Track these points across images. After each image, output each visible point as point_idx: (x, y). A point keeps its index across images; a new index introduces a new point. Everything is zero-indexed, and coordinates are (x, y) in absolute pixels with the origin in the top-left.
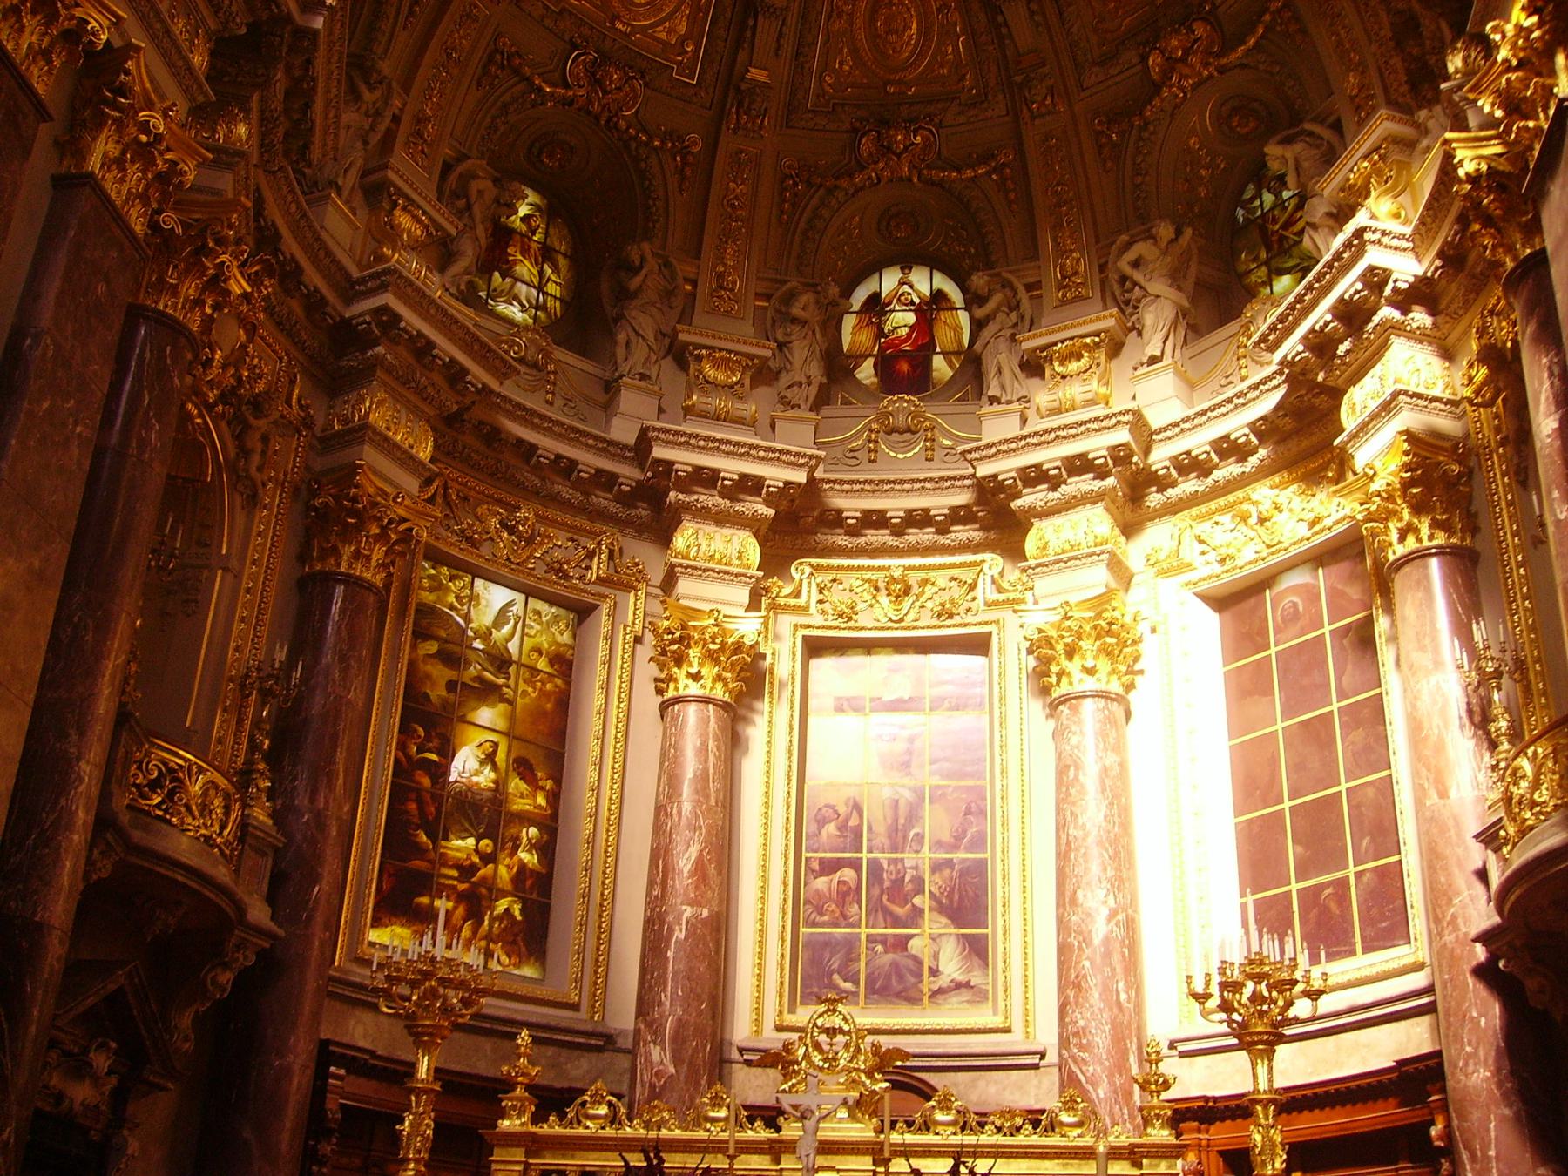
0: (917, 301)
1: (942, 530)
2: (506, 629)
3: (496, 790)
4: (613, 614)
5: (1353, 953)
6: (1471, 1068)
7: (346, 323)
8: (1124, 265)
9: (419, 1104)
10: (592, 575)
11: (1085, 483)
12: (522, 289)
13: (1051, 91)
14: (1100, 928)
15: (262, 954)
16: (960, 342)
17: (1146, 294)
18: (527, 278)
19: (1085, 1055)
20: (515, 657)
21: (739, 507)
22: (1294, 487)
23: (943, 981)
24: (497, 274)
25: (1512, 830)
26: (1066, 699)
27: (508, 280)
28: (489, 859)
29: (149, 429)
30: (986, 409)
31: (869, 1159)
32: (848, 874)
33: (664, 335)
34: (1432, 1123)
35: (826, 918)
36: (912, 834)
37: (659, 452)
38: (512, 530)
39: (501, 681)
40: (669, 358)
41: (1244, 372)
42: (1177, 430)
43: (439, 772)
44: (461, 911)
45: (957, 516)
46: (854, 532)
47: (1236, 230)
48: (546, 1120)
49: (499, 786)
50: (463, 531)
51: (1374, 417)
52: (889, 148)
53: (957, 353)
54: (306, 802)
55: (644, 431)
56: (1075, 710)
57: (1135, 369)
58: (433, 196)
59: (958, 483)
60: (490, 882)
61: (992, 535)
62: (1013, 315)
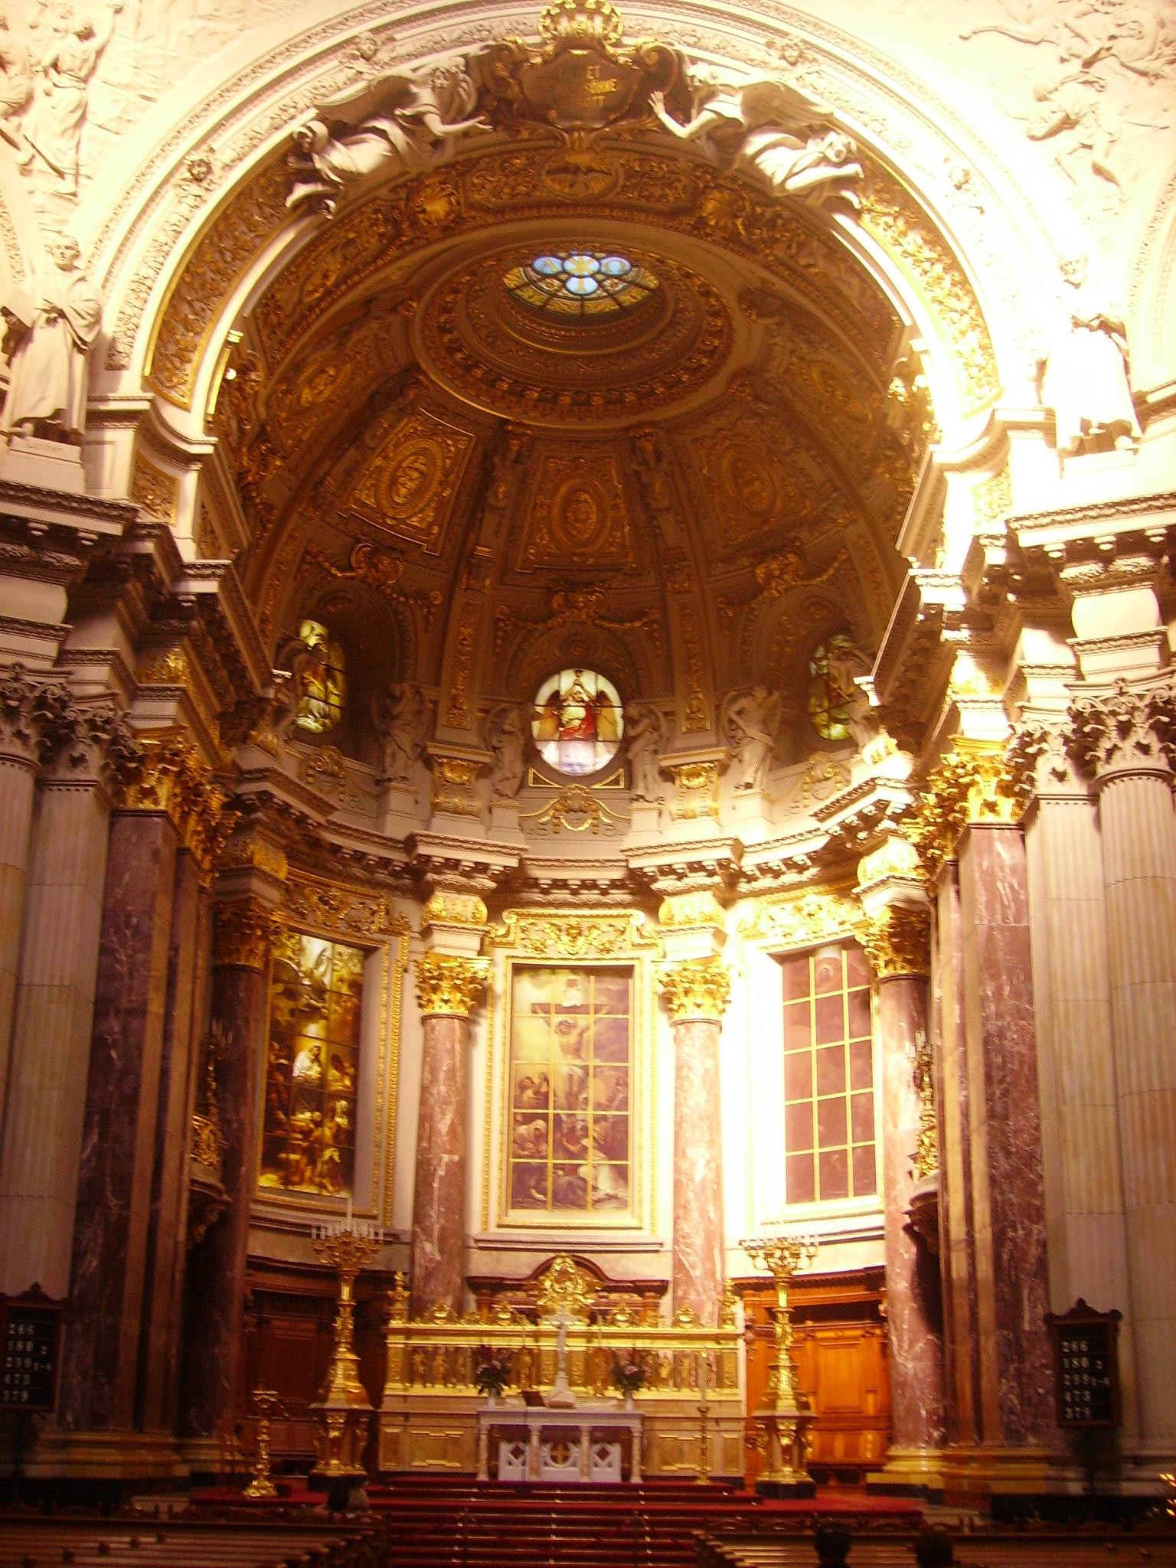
0: (586, 699)
2: (322, 969)
5: (846, 1195)
11: (700, 878)
13: (689, 577)
14: (700, 1173)
15: (222, 1214)
16: (615, 733)
17: (746, 736)
22: (831, 897)
23: (600, 1195)
26: (683, 1023)
28: (319, 1124)
30: (636, 805)
32: (540, 1124)
34: (880, 1302)
37: (423, 850)
38: (326, 903)
39: (320, 1005)
43: (288, 1070)
44: (304, 1160)
45: (614, 884)
47: (809, 680)
49: (323, 1074)
51: (877, 885)
61: (638, 898)
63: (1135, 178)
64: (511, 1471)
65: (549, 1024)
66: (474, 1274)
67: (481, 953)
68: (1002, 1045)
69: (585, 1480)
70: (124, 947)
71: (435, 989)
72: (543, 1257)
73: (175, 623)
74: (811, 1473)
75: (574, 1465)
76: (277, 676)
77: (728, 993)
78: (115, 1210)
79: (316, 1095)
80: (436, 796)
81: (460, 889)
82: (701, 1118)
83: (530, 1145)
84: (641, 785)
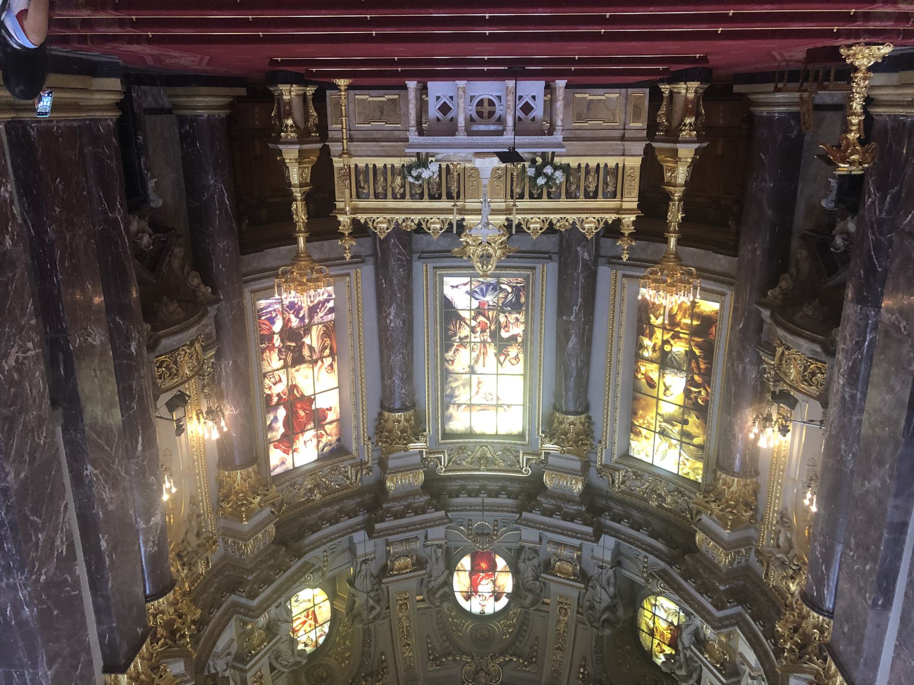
0: (477, 596)
3: (663, 373)
4: (612, 454)
6: (226, 247)
7: (740, 602)
9: (674, 226)
10: (622, 473)
11: (397, 506)
12: (664, 616)
16: (458, 574)
17: (368, 593)
18: (661, 621)
19: (399, 256)
20: (657, 435)
24: (676, 624)
25: (197, 346)
27: (670, 620)
29: (821, 553)
30: (443, 542)
31: (467, 207)
32: (504, 334)
33: (592, 587)
35: (515, 316)
36: (478, 352)
37: (590, 530)
38: (660, 495)
39: (664, 424)
40: (589, 575)
41: (325, 554)
42: (354, 529)
43: (691, 382)
44: (678, 318)
46: (483, 488)
48: (613, 221)
49: (662, 374)
50: (683, 496)
54: (748, 367)
55: (597, 541)
56: (403, 404)
57: (375, 558)
58: (703, 667)
59: (455, 508)
60: (665, 331)
62: (430, 586)
64: (533, 89)
65: (498, 398)
66: (551, 236)
67: (547, 454)
69: (462, 83)
71: (578, 434)
74: (271, 94)
75: (472, 98)
77: (376, 428)
79: (665, 361)
80: (579, 557)
81: (564, 497)
83: (512, 321)
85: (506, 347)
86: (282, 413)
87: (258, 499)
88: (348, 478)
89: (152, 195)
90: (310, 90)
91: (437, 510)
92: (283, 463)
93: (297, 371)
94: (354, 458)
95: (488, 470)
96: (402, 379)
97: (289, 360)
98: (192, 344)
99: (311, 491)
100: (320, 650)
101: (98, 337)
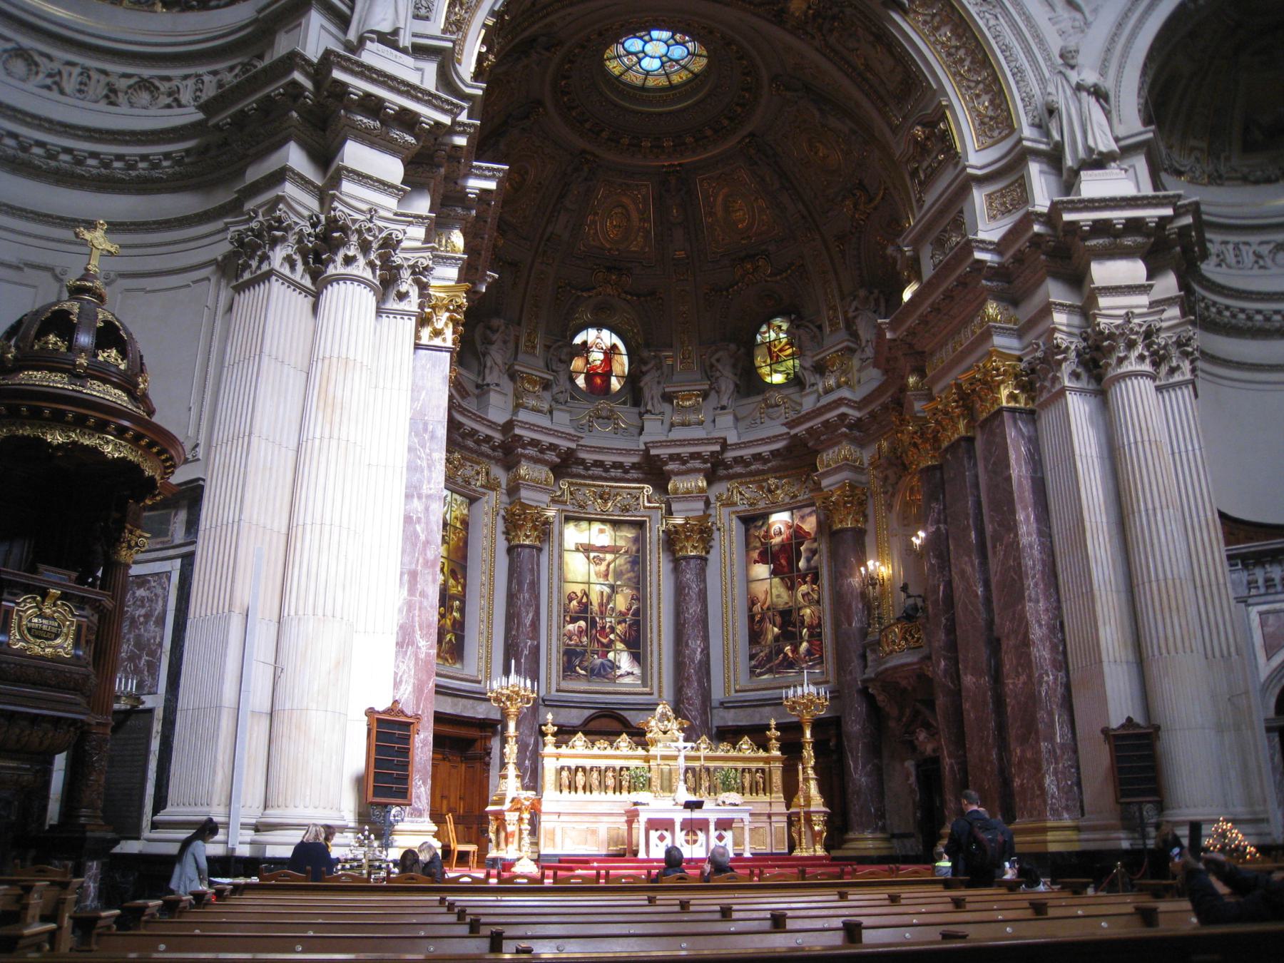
1: (626, 472)
8: (713, 360)
9: (512, 742)
11: (697, 464)
16: (624, 372)
17: (722, 375)
21: (546, 457)
32: (582, 623)
34: (829, 740)
37: (517, 431)
45: (634, 466)
52: (609, 282)
53: (622, 377)
56: (688, 563)
57: (715, 409)
62: (659, 372)
63: (1095, 11)
68: (1032, 554)
70: (423, 447)
72: (587, 713)
73: (459, 210)
76: (489, 276)
78: (424, 649)
81: (537, 461)
82: (698, 621)
84: (650, 404)
85: (581, 612)
86: (802, 564)
87: (833, 499)
88: (741, 493)
89: (913, 770)
90: (797, 853)
91: (658, 456)
92: (802, 518)
93: (787, 603)
94: (733, 512)
95: (602, 486)
96: (690, 588)
97: (795, 615)
98: (891, 652)
99: (777, 488)
100: (767, 320)
101: (968, 680)
